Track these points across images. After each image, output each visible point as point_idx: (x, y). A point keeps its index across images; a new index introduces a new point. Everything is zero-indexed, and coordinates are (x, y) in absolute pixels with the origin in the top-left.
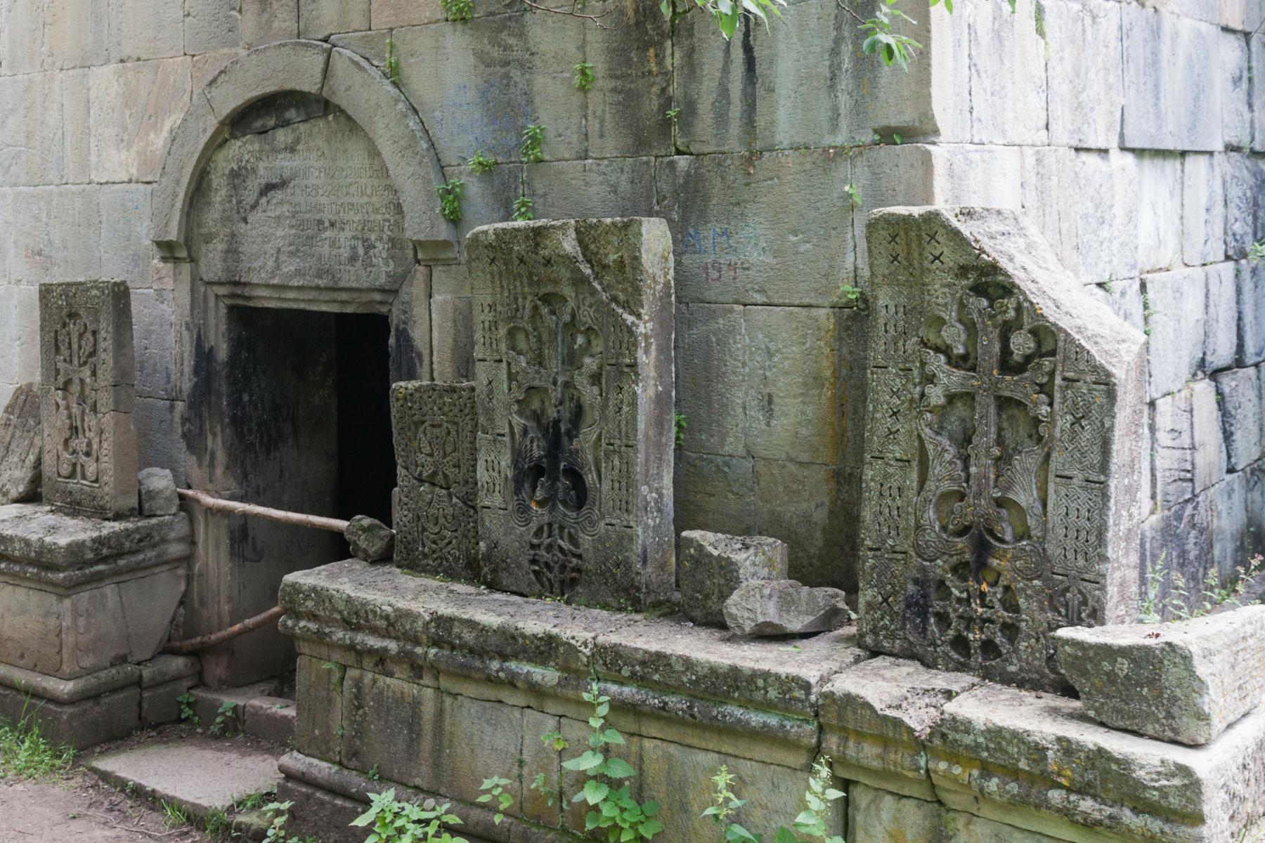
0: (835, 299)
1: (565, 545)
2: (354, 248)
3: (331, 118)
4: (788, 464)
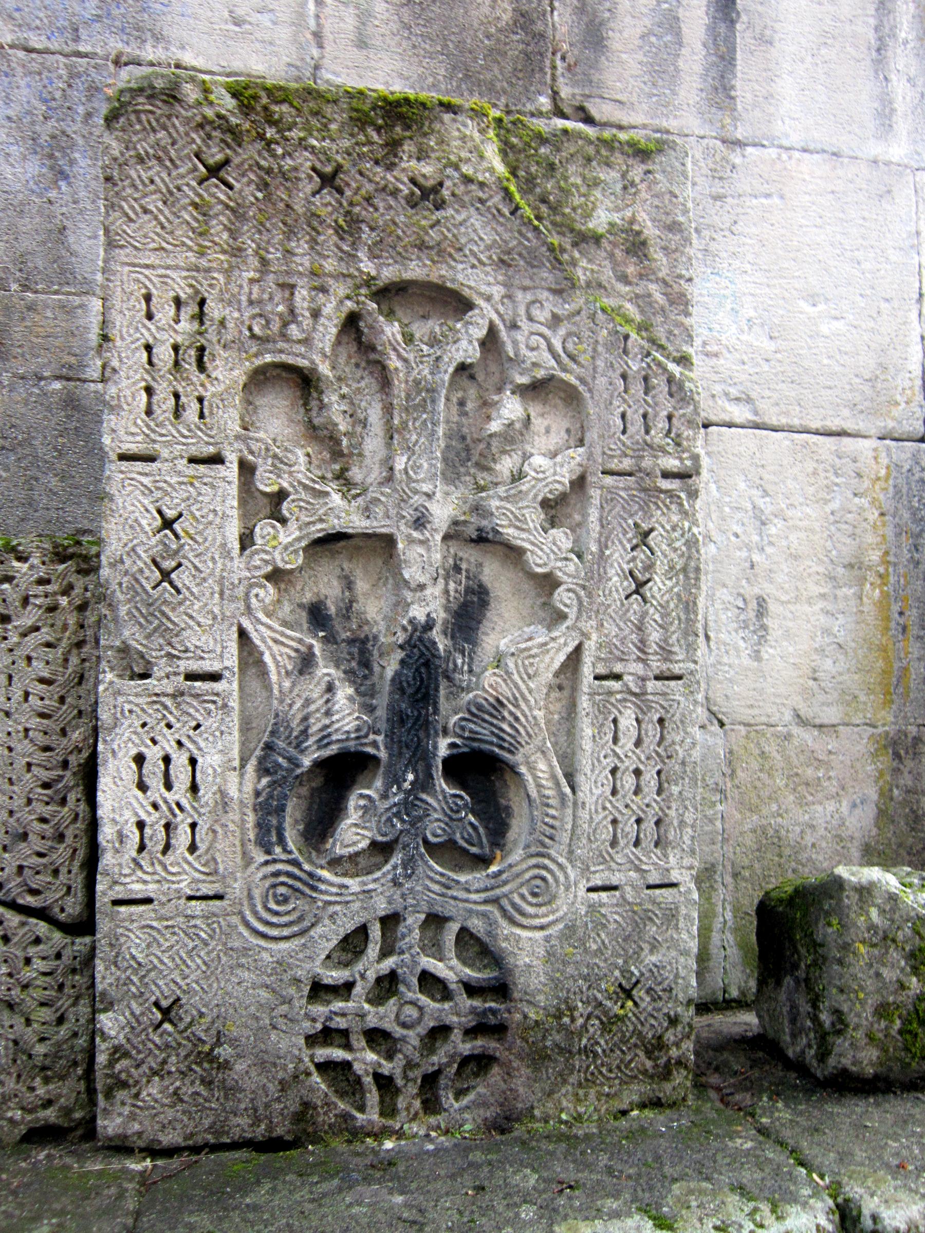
0: (891, 424)
1: (450, 969)
4: (796, 730)
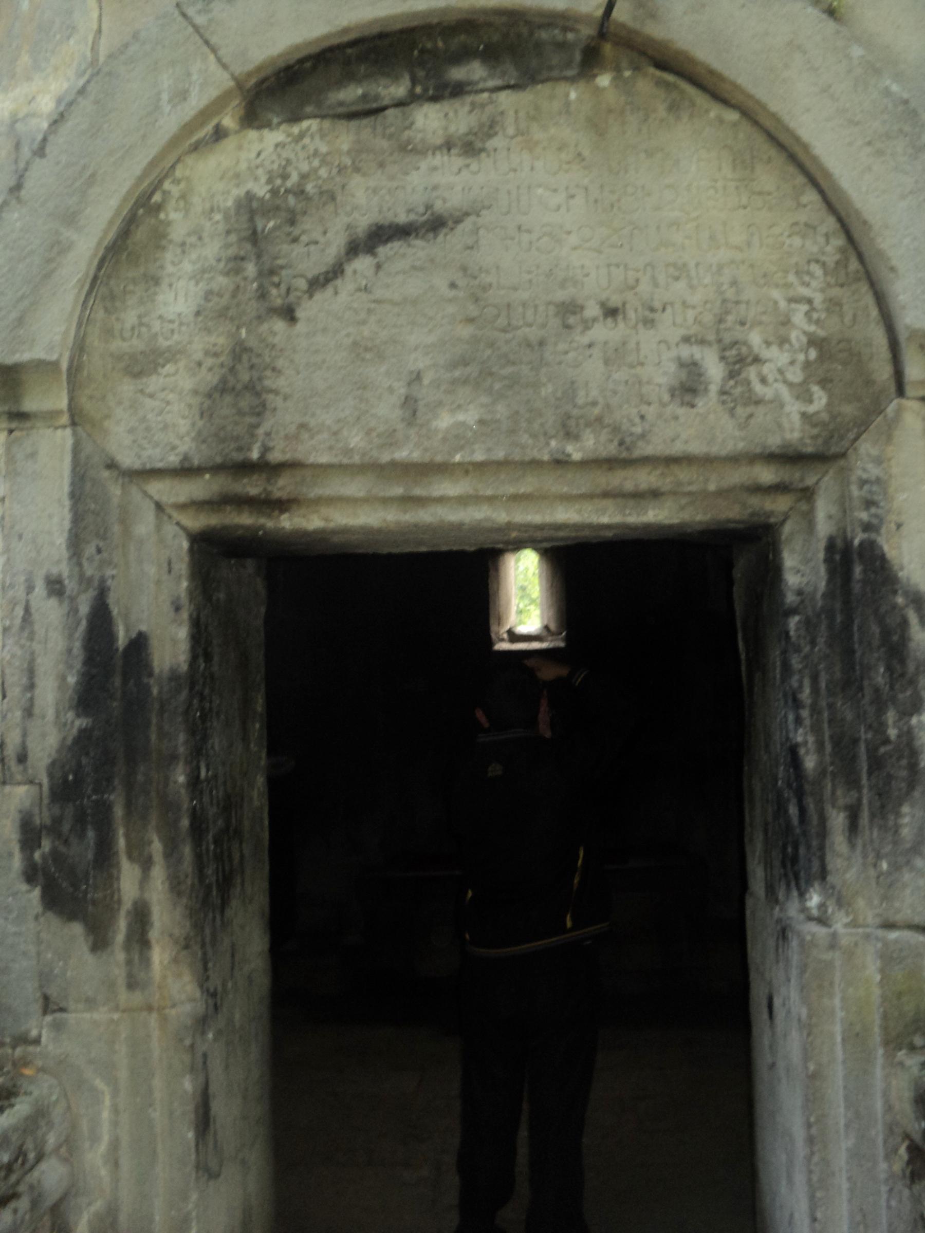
2: (692, 368)
3: (604, 80)
